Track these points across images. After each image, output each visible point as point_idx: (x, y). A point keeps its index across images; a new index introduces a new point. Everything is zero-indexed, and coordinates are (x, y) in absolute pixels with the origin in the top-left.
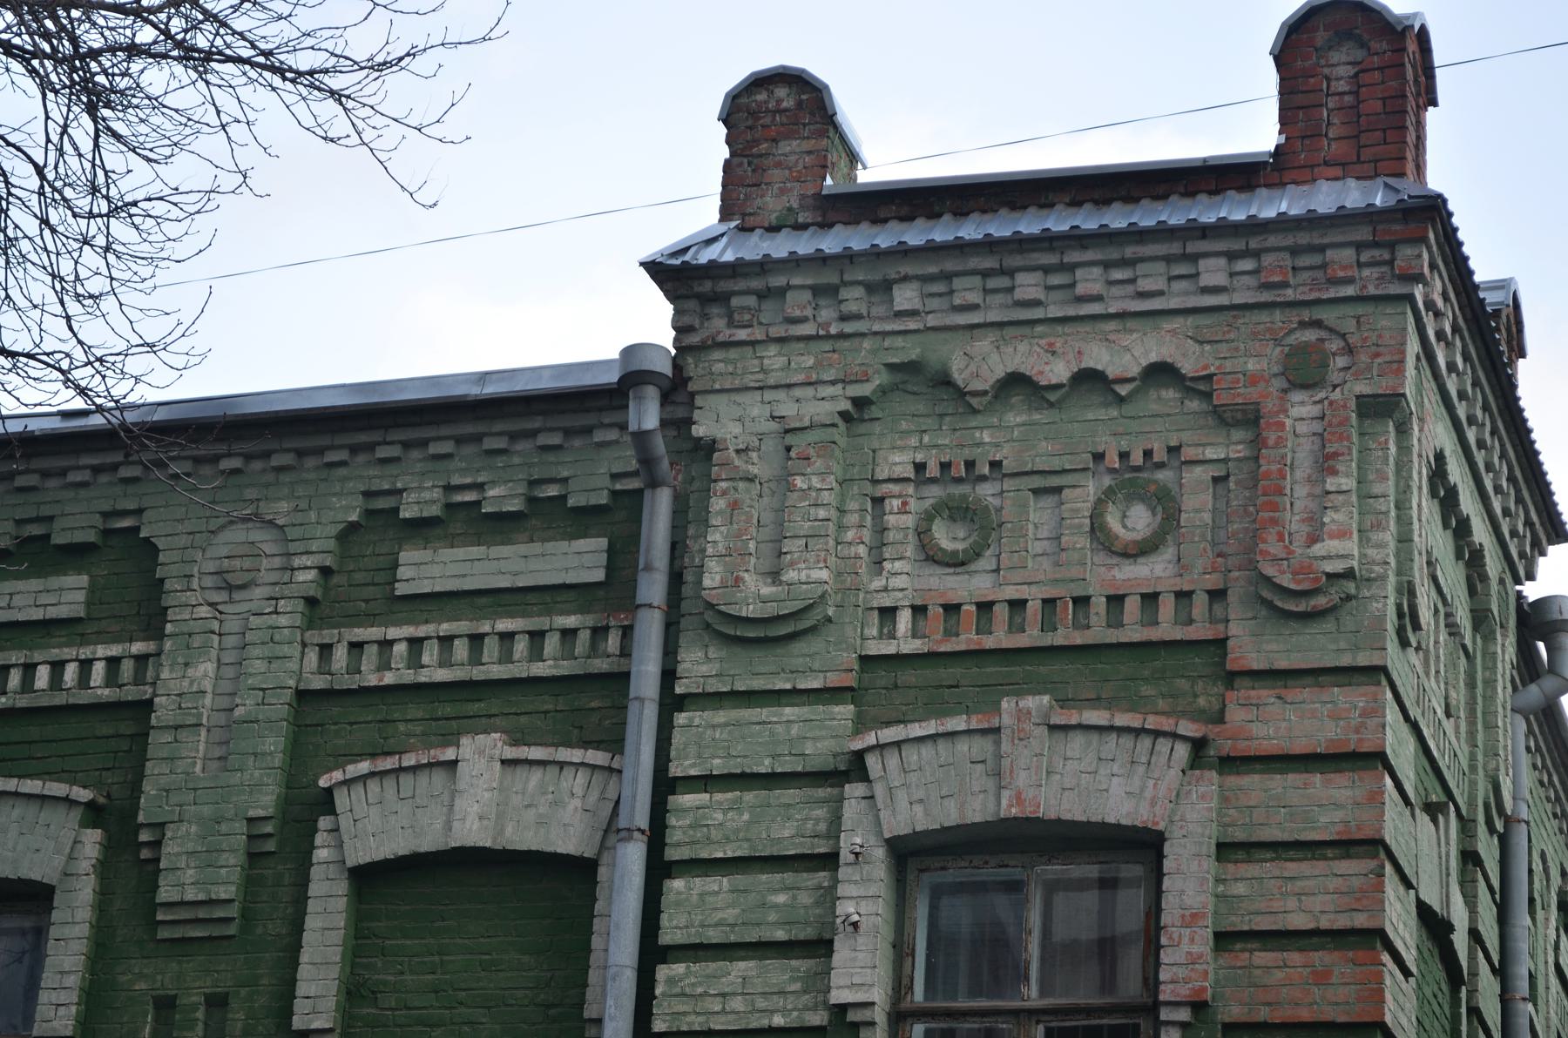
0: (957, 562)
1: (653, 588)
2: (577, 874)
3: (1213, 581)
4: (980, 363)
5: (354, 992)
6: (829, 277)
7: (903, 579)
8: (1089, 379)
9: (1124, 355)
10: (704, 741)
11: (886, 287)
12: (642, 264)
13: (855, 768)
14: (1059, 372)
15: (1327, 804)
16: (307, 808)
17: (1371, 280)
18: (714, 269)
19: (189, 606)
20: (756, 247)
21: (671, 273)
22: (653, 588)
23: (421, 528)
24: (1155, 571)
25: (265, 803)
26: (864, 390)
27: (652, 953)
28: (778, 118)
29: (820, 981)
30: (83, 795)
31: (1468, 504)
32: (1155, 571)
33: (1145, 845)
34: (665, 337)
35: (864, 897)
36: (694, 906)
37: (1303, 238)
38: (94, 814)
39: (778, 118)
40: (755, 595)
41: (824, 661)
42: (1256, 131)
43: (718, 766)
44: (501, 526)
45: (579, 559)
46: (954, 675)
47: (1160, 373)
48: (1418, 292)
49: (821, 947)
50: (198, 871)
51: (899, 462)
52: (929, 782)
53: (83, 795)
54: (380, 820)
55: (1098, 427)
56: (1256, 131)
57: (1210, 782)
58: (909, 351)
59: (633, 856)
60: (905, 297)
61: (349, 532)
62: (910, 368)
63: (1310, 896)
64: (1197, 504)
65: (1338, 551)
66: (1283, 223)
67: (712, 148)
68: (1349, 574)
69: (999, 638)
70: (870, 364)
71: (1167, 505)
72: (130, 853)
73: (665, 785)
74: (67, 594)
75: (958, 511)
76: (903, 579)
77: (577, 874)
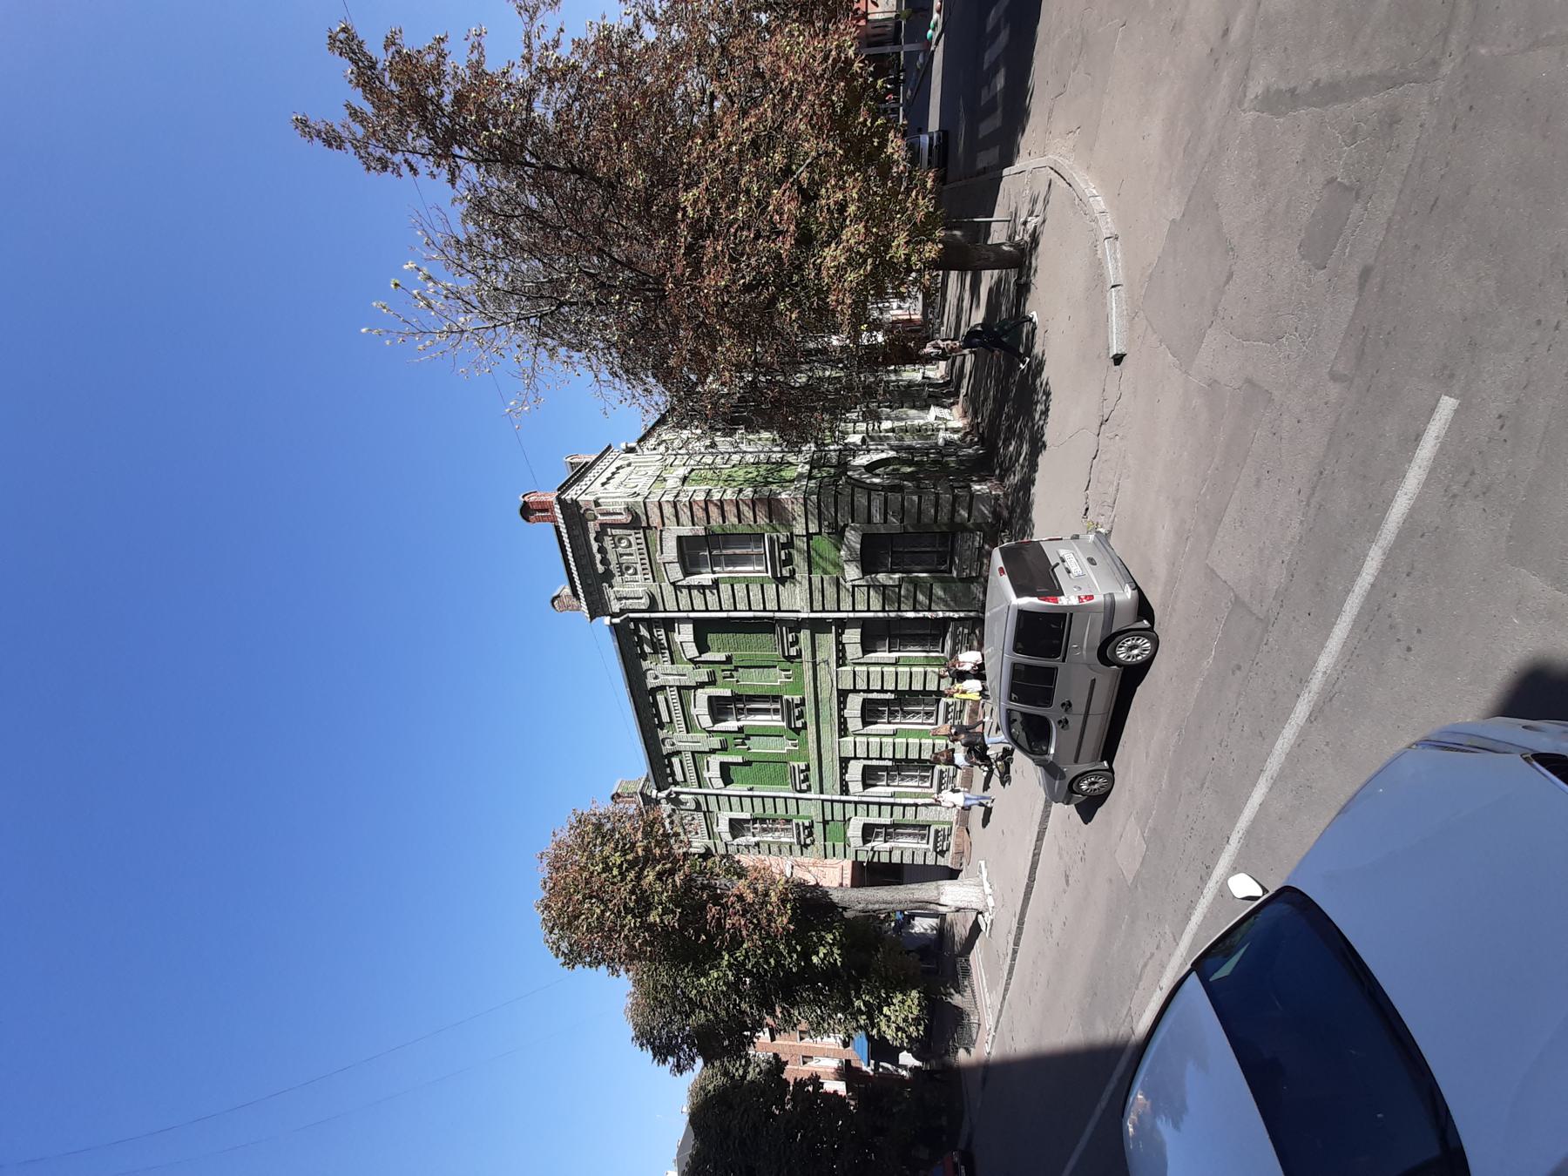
1: (647, 615)
2: (695, 621)
7: (639, 577)
13: (673, 584)
22: (647, 615)
27: (707, 610)
31: (608, 474)
33: (679, 538)
35: (694, 580)
42: (551, 525)
46: (653, 569)
54: (692, 651)
59: (692, 615)
75: (628, 568)
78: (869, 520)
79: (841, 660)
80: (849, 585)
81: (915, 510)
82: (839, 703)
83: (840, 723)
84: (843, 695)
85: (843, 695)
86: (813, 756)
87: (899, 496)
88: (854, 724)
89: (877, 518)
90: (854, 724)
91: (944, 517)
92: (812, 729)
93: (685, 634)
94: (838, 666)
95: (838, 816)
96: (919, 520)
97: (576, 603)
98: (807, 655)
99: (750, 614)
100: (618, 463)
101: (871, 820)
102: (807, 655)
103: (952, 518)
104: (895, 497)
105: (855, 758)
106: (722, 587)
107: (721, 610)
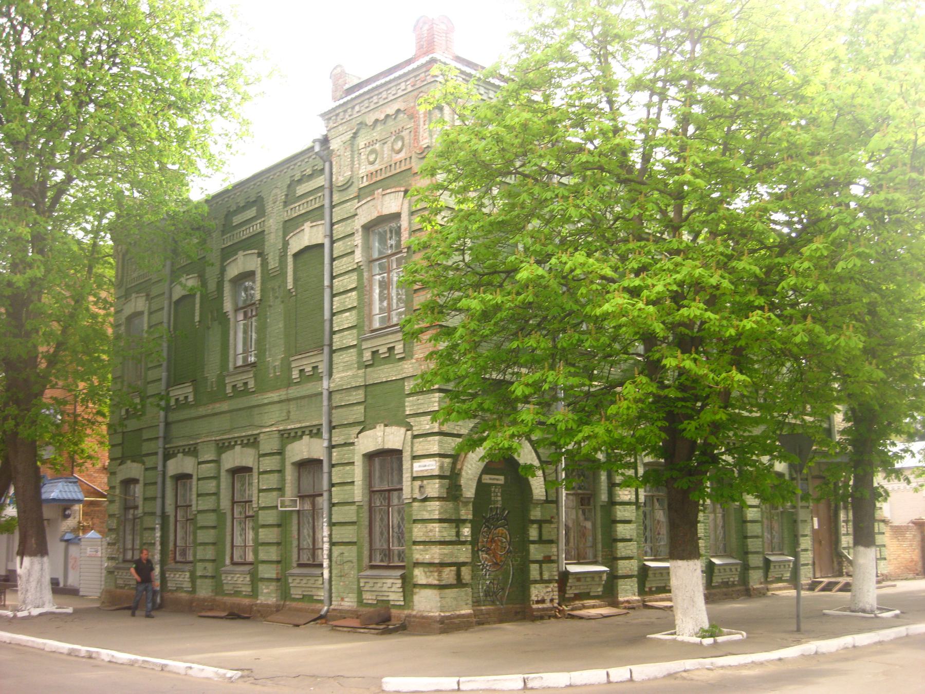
0: (372, 163)
3: (409, 155)
4: (370, 120)
5: (296, 280)
6: (344, 108)
8: (387, 116)
9: (391, 110)
11: (353, 108)
12: (322, 115)
14: (382, 117)
16: (286, 244)
17: (429, 79)
18: (330, 112)
23: (300, 181)
24: (402, 155)
26: (354, 131)
27: (333, 260)
30: (256, 251)
32: (402, 155)
33: (397, 216)
36: (339, 248)
37: (415, 74)
38: (260, 255)
39: (338, 76)
41: (353, 192)
43: (339, 218)
47: (398, 111)
49: (353, 252)
50: (273, 263)
51: (362, 145)
52: (366, 214)
53: (256, 251)
55: (391, 125)
58: (359, 120)
59: (327, 242)
60: (357, 108)
61: (289, 186)
62: (361, 123)
68: (428, 147)
71: (402, 139)
72: (264, 263)
73: (332, 225)
74: (251, 213)
75: (373, 151)
76: (364, 169)
77: (322, 245)
78: (415, 458)
89: (421, 467)
94: (282, 433)
95: (146, 448)
96: (415, 521)
97: (339, 94)
98: (294, 392)
99: (327, 315)
102: (294, 392)
103: (417, 564)
106: (354, 276)
107: (332, 278)
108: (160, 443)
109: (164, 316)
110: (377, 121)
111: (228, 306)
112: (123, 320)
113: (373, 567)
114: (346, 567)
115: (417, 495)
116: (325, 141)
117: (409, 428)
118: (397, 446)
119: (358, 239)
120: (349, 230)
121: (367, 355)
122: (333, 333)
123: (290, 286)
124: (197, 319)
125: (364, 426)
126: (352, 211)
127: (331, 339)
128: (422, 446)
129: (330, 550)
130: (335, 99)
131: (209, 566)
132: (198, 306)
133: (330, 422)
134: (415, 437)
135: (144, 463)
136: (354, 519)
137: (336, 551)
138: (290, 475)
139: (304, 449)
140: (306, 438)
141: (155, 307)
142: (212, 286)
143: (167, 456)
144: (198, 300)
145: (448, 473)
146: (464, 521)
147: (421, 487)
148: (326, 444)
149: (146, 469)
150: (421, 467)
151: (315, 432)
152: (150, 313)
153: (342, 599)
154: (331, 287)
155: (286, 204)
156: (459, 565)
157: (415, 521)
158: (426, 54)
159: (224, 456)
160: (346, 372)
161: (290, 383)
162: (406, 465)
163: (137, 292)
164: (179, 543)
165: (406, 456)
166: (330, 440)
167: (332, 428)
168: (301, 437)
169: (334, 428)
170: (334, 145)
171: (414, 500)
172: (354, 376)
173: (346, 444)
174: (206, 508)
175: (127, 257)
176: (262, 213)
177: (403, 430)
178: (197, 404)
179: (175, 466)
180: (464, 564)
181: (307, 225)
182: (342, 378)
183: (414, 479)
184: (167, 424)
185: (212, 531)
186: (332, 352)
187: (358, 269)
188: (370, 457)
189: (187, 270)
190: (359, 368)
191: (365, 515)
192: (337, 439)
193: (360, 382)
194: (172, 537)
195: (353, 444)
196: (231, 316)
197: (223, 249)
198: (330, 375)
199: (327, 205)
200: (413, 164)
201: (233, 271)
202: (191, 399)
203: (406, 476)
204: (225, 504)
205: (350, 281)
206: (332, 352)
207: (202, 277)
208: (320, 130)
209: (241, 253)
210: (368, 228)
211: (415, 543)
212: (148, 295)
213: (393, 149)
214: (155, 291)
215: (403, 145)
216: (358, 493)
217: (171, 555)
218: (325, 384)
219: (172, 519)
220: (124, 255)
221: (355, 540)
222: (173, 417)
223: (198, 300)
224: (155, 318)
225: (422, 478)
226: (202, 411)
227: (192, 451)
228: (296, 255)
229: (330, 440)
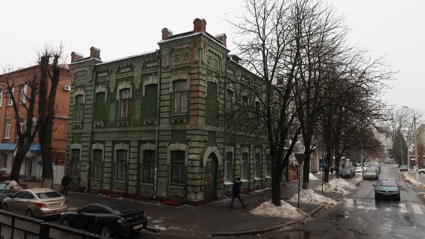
2: (157, 84)
4: (176, 48)
10: (164, 76)
14: (181, 48)
15: (196, 76)
16: (142, 82)
19: (135, 70)
20: (165, 41)
21: (159, 44)
23: (148, 63)
24: (188, 61)
25: (140, 82)
27: (160, 90)
28: (165, 32)
29: (169, 91)
32: (188, 61)
33: (186, 80)
34: (159, 48)
36: (163, 86)
38: (132, 83)
39: (165, 32)
40: (165, 66)
41: (169, 70)
44: (152, 62)
45: (156, 64)
47: (187, 47)
48: (202, 40)
50: (137, 87)
51: (173, 55)
54: (146, 83)
56: (192, 29)
57: (189, 76)
63: (196, 82)
64: (190, 57)
65: (197, 59)
66: (191, 37)
67: (161, 34)
69: (179, 67)
70: (170, 48)
71: (188, 56)
74: (129, 69)
75: (176, 58)
76: (173, 64)
77: (157, 84)
78: (190, 154)
79: (141, 142)
80: (167, 145)
81: (193, 171)
82: (126, 141)
83: (118, 141)
84: (128, 142)
85: (128, 142)
86: (106, 130)
87: (198, 165)
88: (118, 147)
89: (190, 157)
90: (118, 147)
91: (189, 182)
92: (116, 130)
93: (152, 80)
94: (139, 141)
96: (189, 173)
97: (165, 38)
98: (144, 128)
100: (221, 55)
101: (81, 153)
102: (144, 128)
104: (197, 163)
105: (105, 147)
106: (169, 96)
107: (160, 95)
108: (89, 139)
109: (92, 97)
110: (179, 49)
111: (118, 98)
112: (74, 96)
113: (171, 185)
114: (163, 184)
115: (190, 165)
116: (159, 52)
117: (188, 145)
118: (184, 150)
119: (171, 85)
120: (168, 81)
121: (173, 121)
122: (160, 112)
123: (144, 95)
124: (106, 100)
125: (171, 142)
126: (169, 76)
127: (159, 114)
128: (192, 151)
129: (157, 179)
130: (163, 39)
131: (109, 180)
132: (106, 96)
133: (158, 139)
134: (189, 147)
135: (82, 144)
136: (167, 170)
137: (160, 179)
138: (141, 155)
139: (147, 147)
140: (148, 144)
141: (88, 94)
142: (112, 90)
143: (93, 142)
144: (106, 94)
145: (200, 159)
146: (203, 173)
147: (192, 163)
148: (157, 146)
149: (83, 146)
150: (190, 157)
151: (153, 142)
152: (86, 96)
153: (161, 194)
154: (160, 98)
155: (142, 69)
156: (201, 186)
157: (189, 173)
158: (198, 31)
159: (115, 146)
160: (165, 125)
161: (142, 125)
162: (186, 155)
163: (80, 88)
164: (95, 171)
165: (187, 153)
166: (158, 145)
167: (159, 142)
168: (146, 143)
169: (159, 141)
170: (163, 54)
171: (189, 166)
172: (168, 127)
173: (164, 147)
174: (108, 161)
175: (76, 75)
176: (132, 70)
177: (185, 145)
178: (104, 127)
179: (94, 147)
180: (202, 185)
181: (151, 78)
182: (163, 127)
183: (189, 160)
184: (93, 133)
185: (110, 169)
186: (160, 118)
187: (170, 94)
188: (172, 152)
189: (103, 83)
190: (169, 124)
191: (170, 169)
192: (161, 144)
193: (170, 129)
194: (93, 169)
195: (167, 147)
196: (119, 101)
197: (116, 80)
198: (159, 125)
199: (159, 72)
200: (192, 65)
201: (120, 87)
202: (102, 126)
203: (186, 159)
204: (115, 160)
205: (168, 97)
206: (160, 118)
207: (108, 88)
208: (158, 48)
209: (124, 82)
210: (174, 82)
211: (188, 179)
212: (85, 90)
213: (184, 59)
214: (87, 89)
215: (188, 59)
216: (168, 162)
217: (92, 175)
218: (157, 128)
219: (93, 163)
220: (75, 75)
221: (166, 176)
222: (95, 130)
223: (106, 94)
224: (88, 98)
225: (192, 160)
226: (106, 130)
227: (103, 142)
228: (146, 86)
229: (158, 145)
